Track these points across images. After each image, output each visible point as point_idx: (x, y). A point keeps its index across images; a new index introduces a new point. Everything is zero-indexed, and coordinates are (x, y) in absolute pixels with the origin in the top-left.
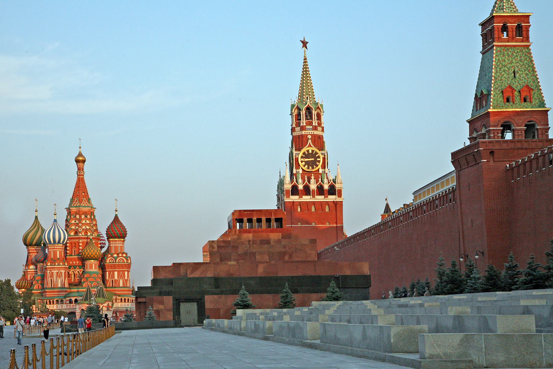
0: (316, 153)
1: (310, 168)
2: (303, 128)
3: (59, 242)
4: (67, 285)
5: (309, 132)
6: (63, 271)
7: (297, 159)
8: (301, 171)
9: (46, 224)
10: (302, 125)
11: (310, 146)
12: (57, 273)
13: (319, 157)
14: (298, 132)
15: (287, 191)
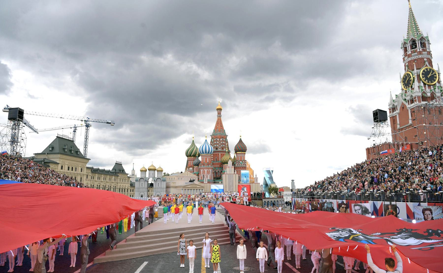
0: (433, 71)
1: (430, 82)
2: (420, 53)
3: (208, 153)
4: (213, 179)
5: (425, 55)
6: (211, 170)
7: (418, 76)
8: (422, 84)
9: (198, 146)
10: (418, 50)
11: (427, 66)
12: (207, 171)
13: (436, 74)
14: (415, 56)
15: (419, 97)
